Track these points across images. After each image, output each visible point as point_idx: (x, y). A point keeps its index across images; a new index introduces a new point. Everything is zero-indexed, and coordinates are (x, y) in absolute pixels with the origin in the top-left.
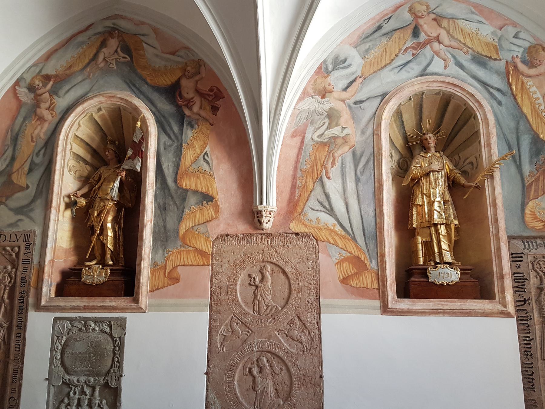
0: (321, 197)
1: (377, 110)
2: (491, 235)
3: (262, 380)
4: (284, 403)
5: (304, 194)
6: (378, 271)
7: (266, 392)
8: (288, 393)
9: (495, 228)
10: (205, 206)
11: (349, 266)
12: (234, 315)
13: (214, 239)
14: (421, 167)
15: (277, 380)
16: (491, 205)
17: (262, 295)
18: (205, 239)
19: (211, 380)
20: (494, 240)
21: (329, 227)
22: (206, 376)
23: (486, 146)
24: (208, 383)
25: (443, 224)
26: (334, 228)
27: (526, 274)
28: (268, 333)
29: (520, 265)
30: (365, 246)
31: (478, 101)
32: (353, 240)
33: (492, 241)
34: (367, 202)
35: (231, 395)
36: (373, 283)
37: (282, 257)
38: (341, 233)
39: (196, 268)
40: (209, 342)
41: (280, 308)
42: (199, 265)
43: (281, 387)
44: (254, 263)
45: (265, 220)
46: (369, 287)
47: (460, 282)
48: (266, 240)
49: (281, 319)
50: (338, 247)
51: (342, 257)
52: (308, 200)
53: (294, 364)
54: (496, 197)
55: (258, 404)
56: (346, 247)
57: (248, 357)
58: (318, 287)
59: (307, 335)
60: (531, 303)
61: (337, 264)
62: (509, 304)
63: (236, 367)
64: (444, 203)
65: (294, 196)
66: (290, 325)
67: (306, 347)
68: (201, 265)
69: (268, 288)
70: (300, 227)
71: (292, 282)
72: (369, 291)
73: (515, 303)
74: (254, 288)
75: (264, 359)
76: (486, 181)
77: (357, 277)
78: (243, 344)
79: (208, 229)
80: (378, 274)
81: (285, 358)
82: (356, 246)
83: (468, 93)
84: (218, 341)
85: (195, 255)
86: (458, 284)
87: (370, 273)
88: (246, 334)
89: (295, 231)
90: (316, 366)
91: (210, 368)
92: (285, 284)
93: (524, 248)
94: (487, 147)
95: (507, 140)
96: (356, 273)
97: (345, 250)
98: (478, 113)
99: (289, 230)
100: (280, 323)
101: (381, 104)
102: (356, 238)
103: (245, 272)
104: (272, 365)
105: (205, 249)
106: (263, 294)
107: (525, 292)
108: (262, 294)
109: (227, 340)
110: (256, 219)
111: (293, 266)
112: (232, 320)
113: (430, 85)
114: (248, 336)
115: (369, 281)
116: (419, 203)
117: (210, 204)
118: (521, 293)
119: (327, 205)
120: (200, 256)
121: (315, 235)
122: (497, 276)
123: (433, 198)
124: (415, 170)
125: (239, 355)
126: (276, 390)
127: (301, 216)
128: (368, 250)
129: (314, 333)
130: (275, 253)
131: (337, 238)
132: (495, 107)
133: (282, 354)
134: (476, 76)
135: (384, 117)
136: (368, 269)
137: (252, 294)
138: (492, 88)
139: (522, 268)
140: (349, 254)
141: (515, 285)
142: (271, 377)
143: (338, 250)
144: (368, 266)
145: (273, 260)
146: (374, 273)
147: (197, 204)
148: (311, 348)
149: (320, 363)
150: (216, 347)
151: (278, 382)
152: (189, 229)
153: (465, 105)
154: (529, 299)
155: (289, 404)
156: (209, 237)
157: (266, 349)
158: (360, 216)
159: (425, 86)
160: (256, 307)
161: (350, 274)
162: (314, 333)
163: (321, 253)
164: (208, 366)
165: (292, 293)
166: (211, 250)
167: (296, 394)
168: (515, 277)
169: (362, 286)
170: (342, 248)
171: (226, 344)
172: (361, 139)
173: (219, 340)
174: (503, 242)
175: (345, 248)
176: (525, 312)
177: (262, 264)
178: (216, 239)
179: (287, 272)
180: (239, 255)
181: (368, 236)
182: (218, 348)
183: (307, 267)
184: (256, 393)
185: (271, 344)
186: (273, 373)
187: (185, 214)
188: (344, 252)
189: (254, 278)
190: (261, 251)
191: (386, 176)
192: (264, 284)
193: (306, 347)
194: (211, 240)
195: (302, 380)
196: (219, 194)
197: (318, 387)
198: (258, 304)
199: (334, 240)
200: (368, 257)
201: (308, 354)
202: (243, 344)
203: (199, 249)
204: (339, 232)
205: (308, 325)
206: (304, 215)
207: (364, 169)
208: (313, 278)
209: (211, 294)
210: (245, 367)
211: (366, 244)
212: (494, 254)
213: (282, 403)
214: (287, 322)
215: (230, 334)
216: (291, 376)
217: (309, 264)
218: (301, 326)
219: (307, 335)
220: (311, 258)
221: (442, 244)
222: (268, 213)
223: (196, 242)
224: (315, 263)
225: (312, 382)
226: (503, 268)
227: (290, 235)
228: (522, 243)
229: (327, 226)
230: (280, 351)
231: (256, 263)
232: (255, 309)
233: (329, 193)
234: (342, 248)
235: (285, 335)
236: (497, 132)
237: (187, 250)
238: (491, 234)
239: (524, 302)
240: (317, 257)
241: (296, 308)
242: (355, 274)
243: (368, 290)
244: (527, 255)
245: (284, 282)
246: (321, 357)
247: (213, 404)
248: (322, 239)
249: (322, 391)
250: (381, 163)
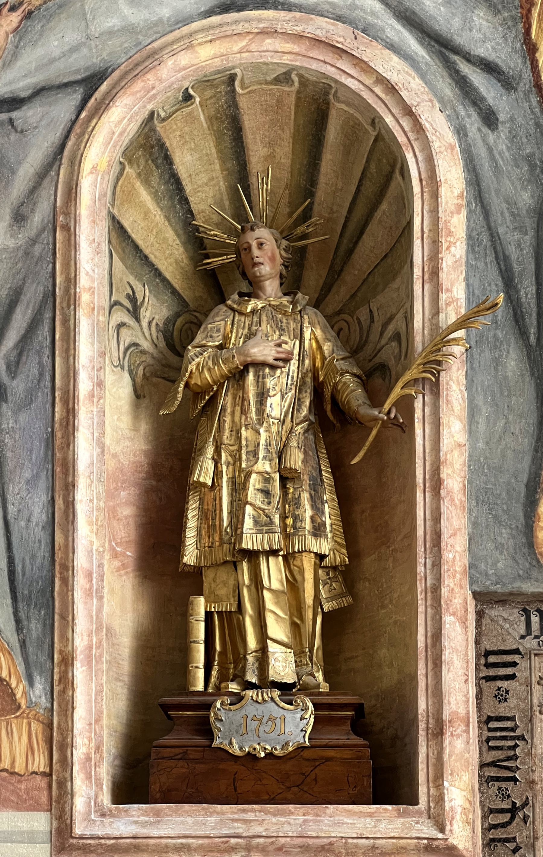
1: (67, 137)
2: (419, 590)
6: (52, 715)
9: (433, 565)
14: (221, 347)
16: (427, 485)
20: (426, 607)
23: (426, 277)
25: (274, 553)
27: (521, 721)
29: (507, 692)
30: (14, 628)
31: (409, 112)
33: (421, 609)
34: (27, 474)
36: (33, 754)
46: (19, 768)
47: (312, 747)
54: (442, 459)
60: (531, 819)
62: (453, 818)
64: (284, 480)
72: (19, 782)
73: (484, 817)
76: (418, 404)
80: (50, 726)
83: (381, 80)
86: (305, 754)
87: (25, 721)
93: (523, 631)
94: (431, 279)
95: (501, 255)
98: (409, 156)
101: (83, 115)
107: (515, 780)
113: (253, 47)
116: (201, 480)
118: (503, 785)
122: (428, 728)
123: (248, 460)
124: (197, 360)
128: (23, 644)
132: (470, 135)
134: (414, 13)
135: (87, 166)
136: (19, 707)
138: (469, 61)
139: (512, 701)
141: (489, 760)
144: (18, 696)
146: (38, 720)
153: (373, 123)
154: (526, 804)
159: (236, 49)
168: (490, 730)
172: (11, 243)
174: (454, 614)
176: (511, 846)
181: (26, 592)
191: (91, 378)
207: (20, 355)
211: (18, 621)
212: (424, 654)
221: (270, 620)
226: (446, 701)
228: (523, 618)
236: (468, 227)
238: (420, 587)
239: (509, 815)
243: (14, 779)
244: (530, 658)
250: (72, 334)
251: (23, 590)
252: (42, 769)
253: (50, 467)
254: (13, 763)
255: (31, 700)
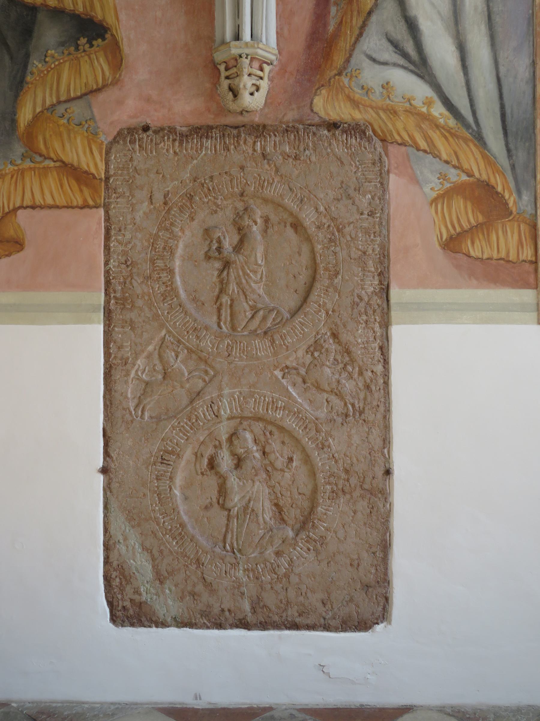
0: (395, 28)
3: (241, 484)
4: (297, 535)
5: (351, 20)
7: (253, 510)
8: (306, 513)
10: (84, 51)
11: (466, 207)
12: (169, 332)
13: (110, 138)
15: (279, 484)
17: (241, 283)
18: (87, 137)
19: (115, 486)
21: (415, 108)
22: (101, 477)
24: (108, 493)
26: (428, 110)
28: (256, 374)
32: (476, 142)
35: (165, 519)
36: (522, 247)
37: (291, 185)
38: (446, 123)
39: (66, 214)
40: (107, 397)
41: (287, 315)
42: (73, 207)
43: (289, 500)
44: (219, 202)
45: (247, 82)
46: (512, 257)
48: (250, 140)
49: (290, 340)
50: (438, 159)
51: (449, 185)
52: (361, 34)
53: (323, 445)
55: (232, 538)
56: (458, 159)
57: (207, 432)
58: (386, 260)
59: (356, 376)
61: (435, 201)
63: (178, 455)
65: (325, 25)
66: (312, 355)
67: (353, 405)
68: (77, 207)
69: (256, 264)
70: (340, 107)
71: (319, 247)
74: (218, 265)
75: (248, 436)
77: (483, 234)
78: (192, 402)
79: (95, 111)
81: (299, 432)
82: (484, 156)
84: (129, 395)
85: (60, 180)
88: (200, 377)
89: (327, 118)
90: (376, 448)
91: (112, 457)
92: (300, 255)
96: (481, 224)
97: (455, 167)
99: (312, 114)
100: (287, 350)
102: (484, 135)
103: (195, 223)
104: (267, 450)
105: (88, 165)
106: (244, 281)
108: (240, 279)
109: (152, 391)
110: (225, 83)
111: (322, 209)
112: (163, 343)
114: (204, 381)
115: (513, 241)
117: (98, 46)
119: (410, 48)
120: (74, 183)
121: (380, 127)
125: (183, 426)
126: (276, 505)
127: (343, 78)
128: (513, 167)
129: (372, 372)
130: (273, 174)
131: (436, 136)
133: (293, 422)
136: (511, 213)
137: (215, 279)
140: (464, 178)
142: (264, 476)
143: (438, 166)
144: (511, 204)
145: (269, 192)
146: (526, 223)
147: (62, 44)
148: (364, 409)
149: (386, 441)
150: (124, 409)
151: (281, 486)
152: (42, 112)
155: (308, 536)
156: (96, 134)
157: (251, 412)
158: (495, 79)
160: (226, 312)
161: (466, 226)
162: (372, 372)
163: (396, 174)
164: (107, 454)
165: (318, 276)
166: (102, 166)
167: (325, 514)
169: (495, 256)
170: (447, 162)
171: (149, 403)
173: (132, 393)
175: (455, 162)
177: (240, 206)
178: (115, 138)
179: (307, 223)
180: (177, 180)
182: (130, 413)
183: (358, 209)
184: (229, 516)
185: (265, 400)
186: (269, 469)
187: (32, 73)
188: (453, 170)
189: (219, 241)
190: (235, 171)
192: (245, 253)
193: (353, 405)
194: (102, 142)
195: (341, 483)
196: (123, 16)
197: (380, 495)
198: (231, 306)
199: (429, 140)
200: (512, 185)
201: (358, 422)
202: (192, 402)
203: (72, 165)
204: (442, 121)
205: (358, 352)
206: (351, 76)
208: (372, 237)
209: (108, 283)
210: (199, 455)
211: (509, 150)
213: (291, 534)
214: (305, 347)
215: (160, 377)
216: (313, 474)
217: (364, 201)
218: (339, 358)
219: (356, 376)
220: (370, 187)
222: (256, 64)
223: (63, 146)
224: (380, 199)
225: (366, 486)
227: (314, 129)
229: (411, 104)
230: (288, 415)
231: (225, 202)
232: (223, 318)
233: (415, 18)
234: (447, 162)
235: (300, 380)
237: (39, 168)
240: (383, 186)
241: (327, 313)
242: (479, 226)
245: (297, 250)
246: (387, 427)
247: (121, 541)
248: (397, 138)
249: (388, 506)
251: (512, 128)
252: (529, 258)
253: (531, 38)
254: (508, 254)
255: (520, 208)
